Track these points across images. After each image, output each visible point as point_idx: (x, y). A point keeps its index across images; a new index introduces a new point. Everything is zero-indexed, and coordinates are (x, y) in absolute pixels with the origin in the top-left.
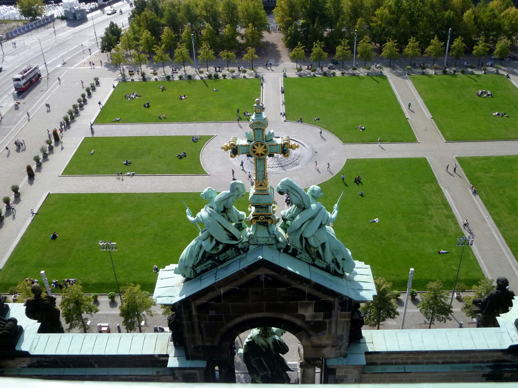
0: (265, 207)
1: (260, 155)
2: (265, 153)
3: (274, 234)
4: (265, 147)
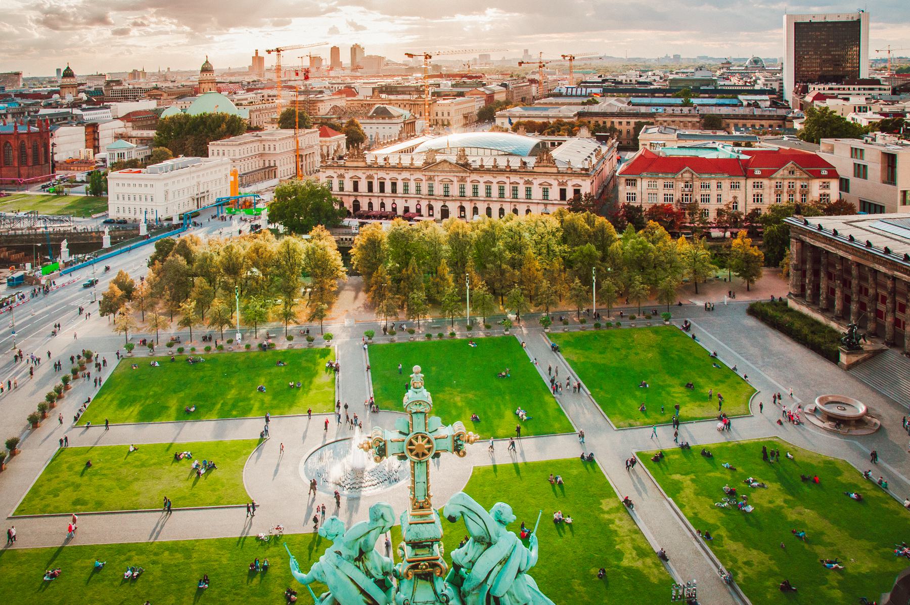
0: (428, 546)
1: (420, 455)
2: (429, 451)
3: (445, 595)
4: (429, 442)
